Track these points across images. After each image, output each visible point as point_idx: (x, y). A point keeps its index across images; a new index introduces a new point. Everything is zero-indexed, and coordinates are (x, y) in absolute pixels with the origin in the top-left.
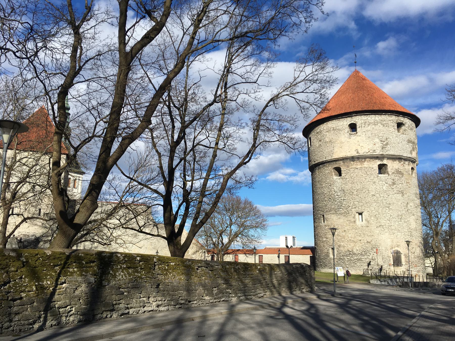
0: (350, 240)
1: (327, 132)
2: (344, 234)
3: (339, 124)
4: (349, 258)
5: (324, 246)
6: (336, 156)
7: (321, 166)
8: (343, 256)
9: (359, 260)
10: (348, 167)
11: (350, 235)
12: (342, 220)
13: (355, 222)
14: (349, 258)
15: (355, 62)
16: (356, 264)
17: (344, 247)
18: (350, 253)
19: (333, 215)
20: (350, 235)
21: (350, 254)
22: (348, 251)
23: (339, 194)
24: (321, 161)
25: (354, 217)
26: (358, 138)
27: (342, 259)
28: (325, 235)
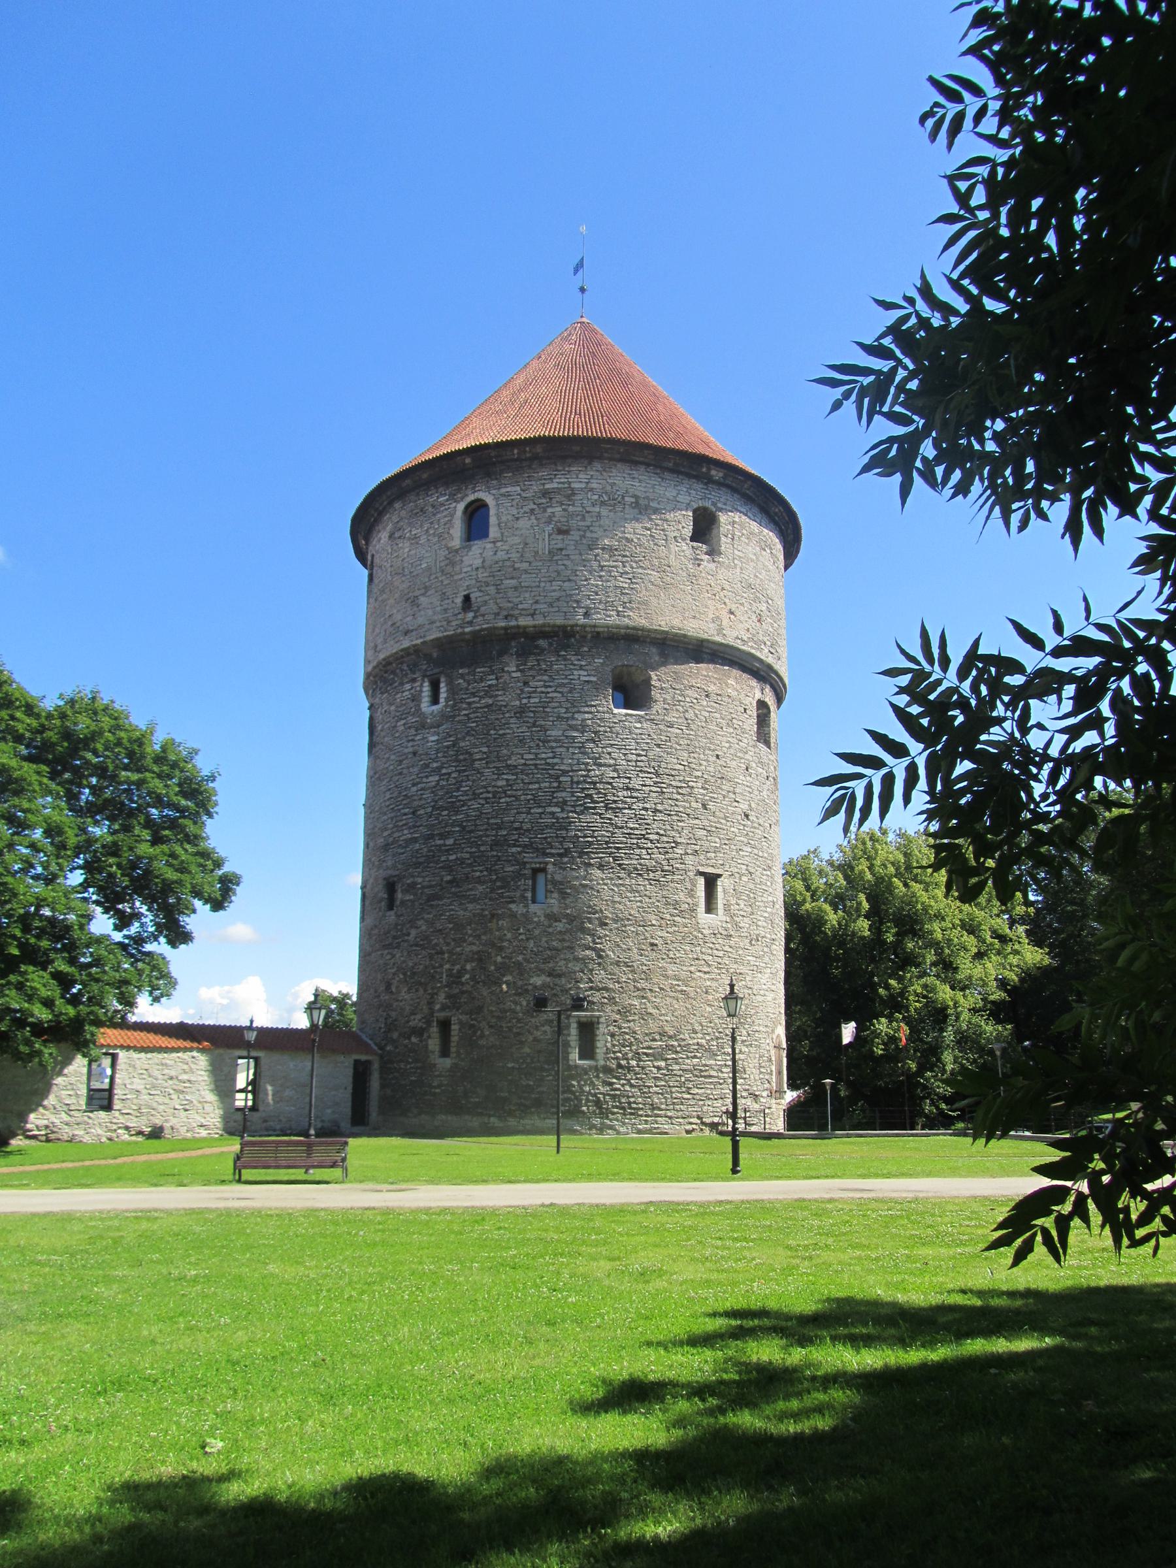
1: (603, 503)
3: (660, 490)
4: (663, 1064)
6: (637, 619)
7: (542, 643)
10: (677, 677)
11: (672, 969)
15: (582, 290)
17: (645, 1015)
19: (597, 873)
22: (663, 1034)
23: (636, 783)
24: (559, 621)
25: (691, 893)
26: (723, 574)
27: (629, 1068)
28: (545, 961)
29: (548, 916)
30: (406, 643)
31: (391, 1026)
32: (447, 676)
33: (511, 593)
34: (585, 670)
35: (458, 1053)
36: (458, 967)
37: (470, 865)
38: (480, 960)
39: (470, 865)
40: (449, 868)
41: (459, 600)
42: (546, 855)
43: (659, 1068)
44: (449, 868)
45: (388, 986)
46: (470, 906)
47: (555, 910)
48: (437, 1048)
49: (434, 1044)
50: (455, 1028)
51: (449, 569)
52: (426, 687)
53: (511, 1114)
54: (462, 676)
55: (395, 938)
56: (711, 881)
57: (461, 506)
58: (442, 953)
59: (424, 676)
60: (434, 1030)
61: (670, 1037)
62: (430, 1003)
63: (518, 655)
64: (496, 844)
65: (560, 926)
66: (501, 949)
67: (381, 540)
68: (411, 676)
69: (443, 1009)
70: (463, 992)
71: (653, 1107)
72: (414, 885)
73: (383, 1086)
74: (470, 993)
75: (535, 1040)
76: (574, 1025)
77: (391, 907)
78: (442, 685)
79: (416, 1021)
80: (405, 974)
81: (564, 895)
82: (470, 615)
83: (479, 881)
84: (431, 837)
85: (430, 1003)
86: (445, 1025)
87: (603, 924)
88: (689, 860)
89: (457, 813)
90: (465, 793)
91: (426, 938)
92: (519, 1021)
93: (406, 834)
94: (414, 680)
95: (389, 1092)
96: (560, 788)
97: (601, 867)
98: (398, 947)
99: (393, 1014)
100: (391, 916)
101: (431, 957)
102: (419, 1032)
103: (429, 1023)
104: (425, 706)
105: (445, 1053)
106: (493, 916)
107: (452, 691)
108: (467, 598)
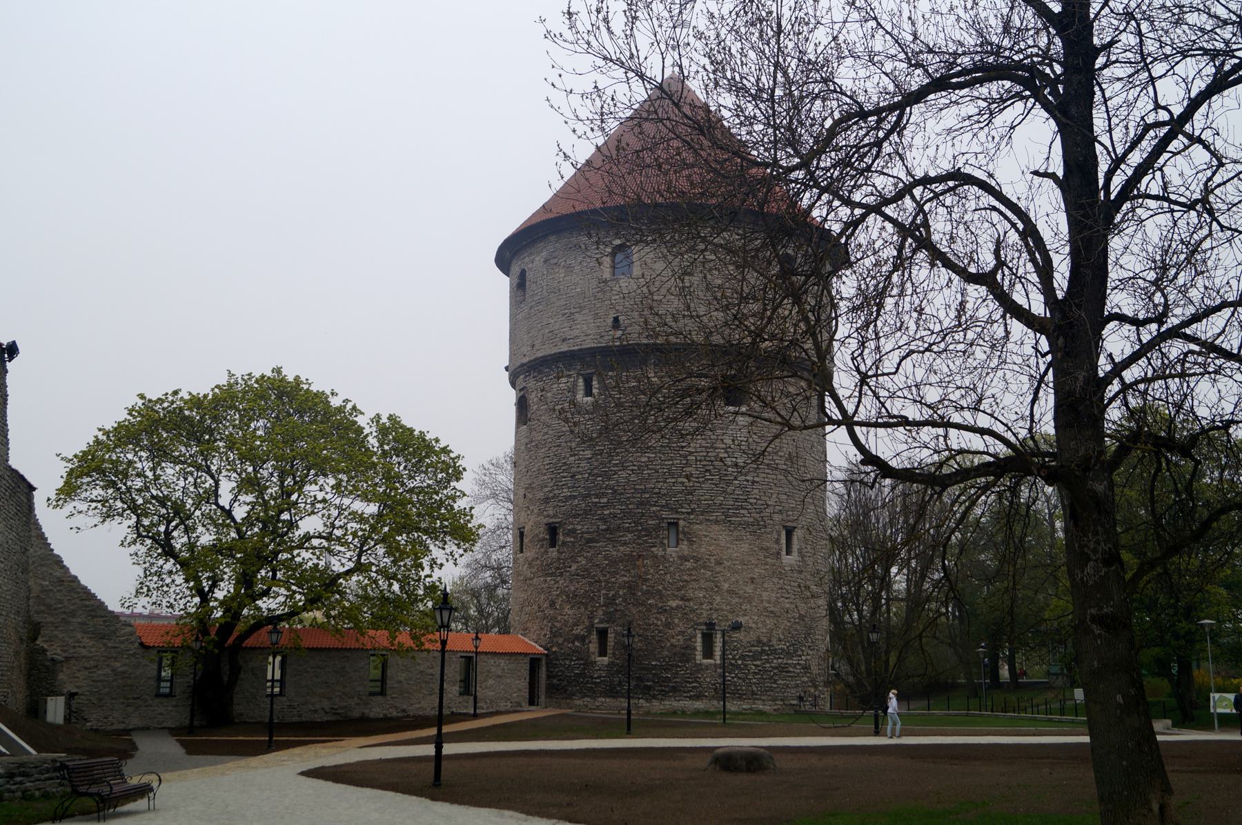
0: (765, 608)
2: (749, 589)
4: (758, 663)
5: (668, 625)
8: (743, 657)
9: (782, 669)
11: (765, 595)
12: (745, 547)
13: (779, 553)
14: (758, 663)
16: (775, 682)
18: (763, 648)
19: (716, 527)
20: (765, 595)
21: (763, 651)
22: (759, 641)
23: (740, 461)
25: (777, 541)
27: (738, 667)
28: (679, 589)
29: (680, 557)
30: (564, 348)
31: (554, 634)
32: (600, 375)
35: (614, 654)
36: (612, 593)
37: (621, 518)
38: (630, 587)
39: (621, 518)
40: (603, 519)
41: (610, 321)
42: (677, 512)
43: (756, 666)
44: (603, 519)
45: (552, 604)
46: (622, 549)
47: (686, 553)
48: (597, 651)
49: (594, 647)
50: (611, 636)
51: (600, 295)
52: (581, 382)
53: (654, 697)
55: (557, 568)
56: (789, 533)
58: (600, 581)
59: (579, 374)
60: (594, 637)
61: (764, 644)
62: (591, 618)
63: (655, 365)
64: (641, 504)
65: (688, 565)
66: (647, 580)
67: (535, 262)
68: (566, 373)
69: (601, 621)
70: (616, 611)
71: (753, 693)
72: (573, 531)
73: (548, 677)
74: (623, 611)
75: (672, 645)
76: (699, 635)
77: (553, 544)
78: (594, 383)
79: (578, 630)
80: (568, 596)
81: (691, 542)
82: (619, 333)
83: (628, 530)
84: (589, 495)
85: (591, 618)
86: (603, 634)
87: (719, 563)
88: (777, 517)
89: (609, 479)
90: (616, 465)
91: (587, 570)
92: (660, 632)
93: (566, 492)
94: (569, 376)
95: (555, 681)
96: (688, 464)
97: (717, 522)
98: (561, 574)
99: (558, 625)
100: (553, 553)
101: (590, 584)
102: (582, 639)
103: (590, 632)
105: (603, 653)
106: (640, 556)
107: (604, 387)
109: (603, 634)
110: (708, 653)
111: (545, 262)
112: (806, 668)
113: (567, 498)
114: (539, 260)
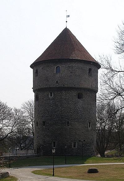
15: (66, 22)
25: (87, 125)
33: (64, 82)
34: (75, 93)
49: (53, 145)
50: (56, 143)
54: (56, 93)
57: (56, 67)
60: (53, 143)
67: (40, 69)
78: (53, 94)
86: (54, 143)
104: (50, 96)
105: (54, 146)
107: (54, 94)
108: (57, 81)
109: (54, 143)
110: (75, 146)
111: (42, 69)
112: (92, 148)
113: (47, 116)
114: (41, 68)
